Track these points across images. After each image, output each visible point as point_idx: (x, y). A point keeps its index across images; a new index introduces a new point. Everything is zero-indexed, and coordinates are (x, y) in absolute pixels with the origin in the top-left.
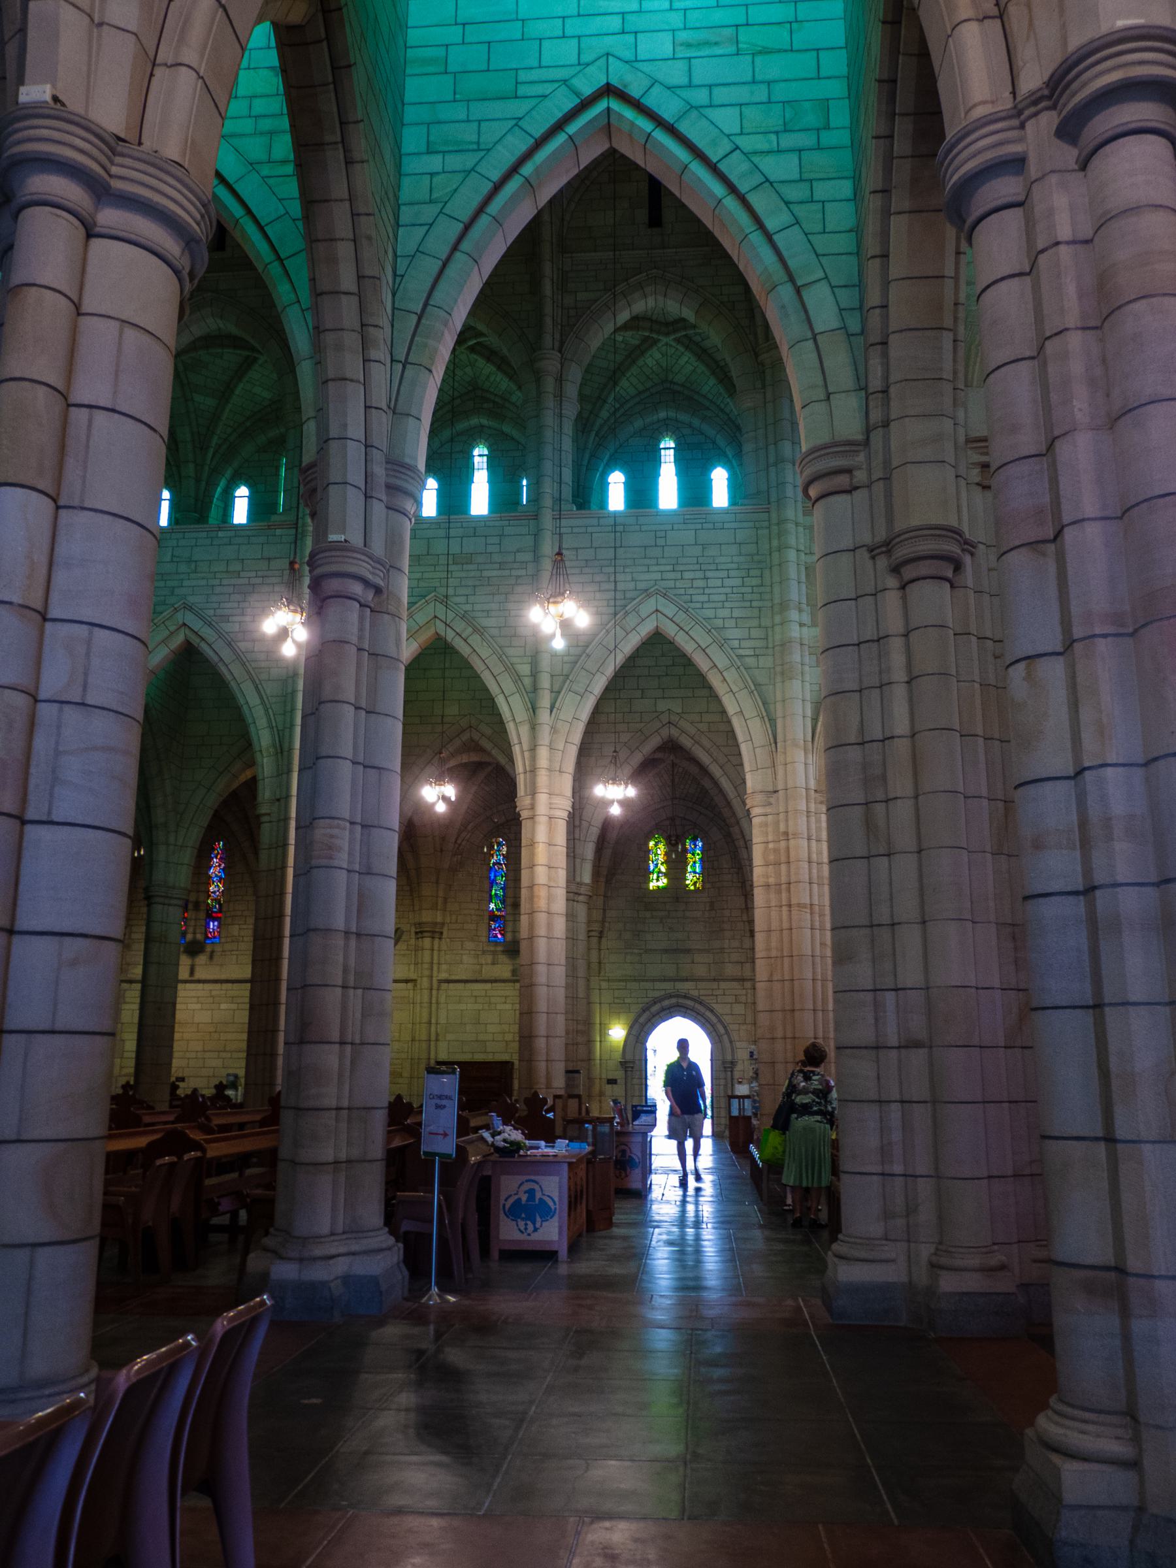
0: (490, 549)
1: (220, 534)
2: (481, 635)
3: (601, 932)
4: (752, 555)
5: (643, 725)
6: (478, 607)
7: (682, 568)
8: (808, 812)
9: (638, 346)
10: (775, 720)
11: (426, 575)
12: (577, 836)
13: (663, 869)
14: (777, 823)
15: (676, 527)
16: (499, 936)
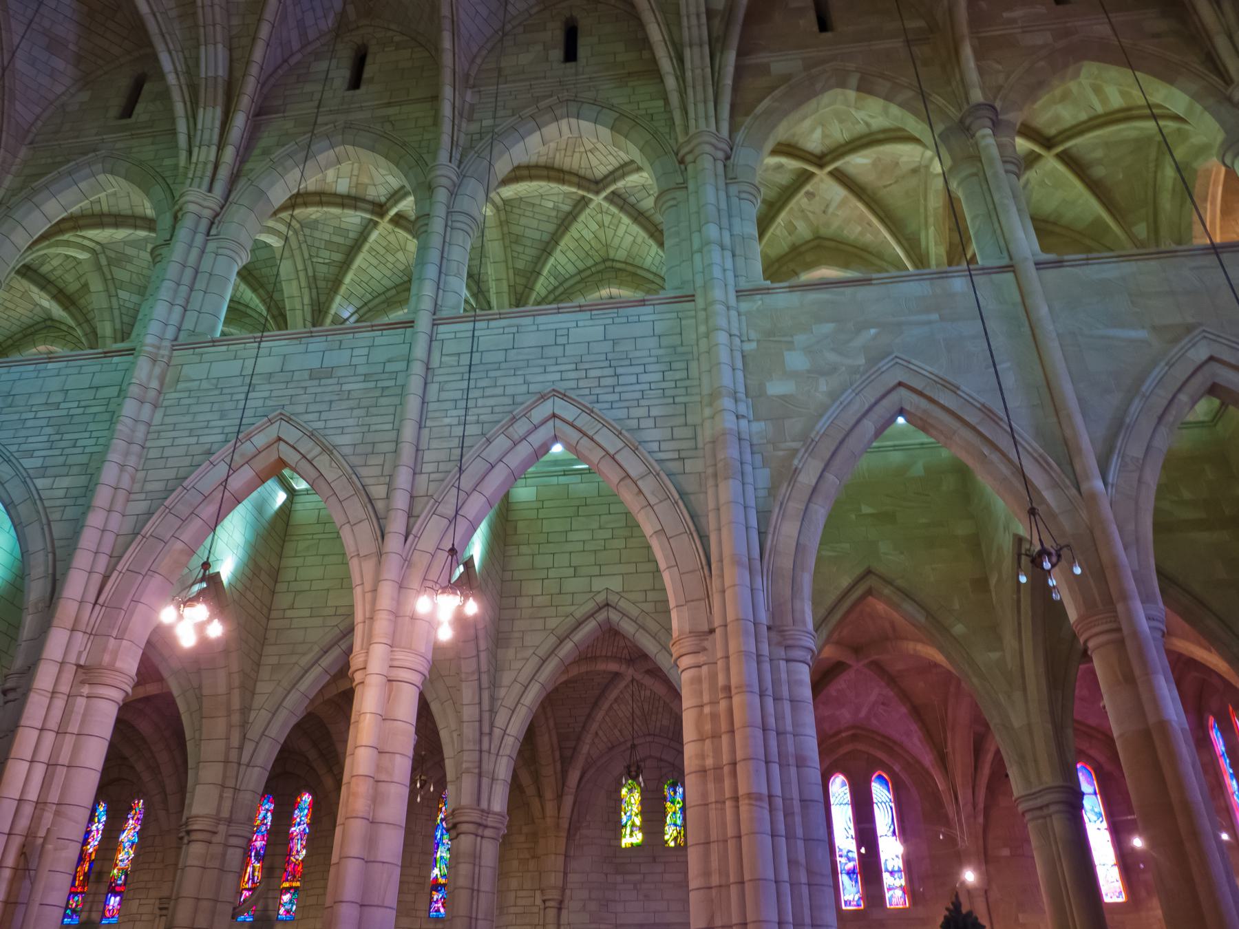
0: (354, 361)
1: (50, 366)
2: (330, 453)
3: (561, 902)
4: (674, 347)
5: (573, 608)
6: (330, 424)
7: (587, 366)
8: (758, 656)
9: (570, 213)
10: (708, 537)
11: (275, 393)
12: (485, 746)
13: (638, 821)
14: (713, 677)
15: (580, 324)
16: (442, 910)
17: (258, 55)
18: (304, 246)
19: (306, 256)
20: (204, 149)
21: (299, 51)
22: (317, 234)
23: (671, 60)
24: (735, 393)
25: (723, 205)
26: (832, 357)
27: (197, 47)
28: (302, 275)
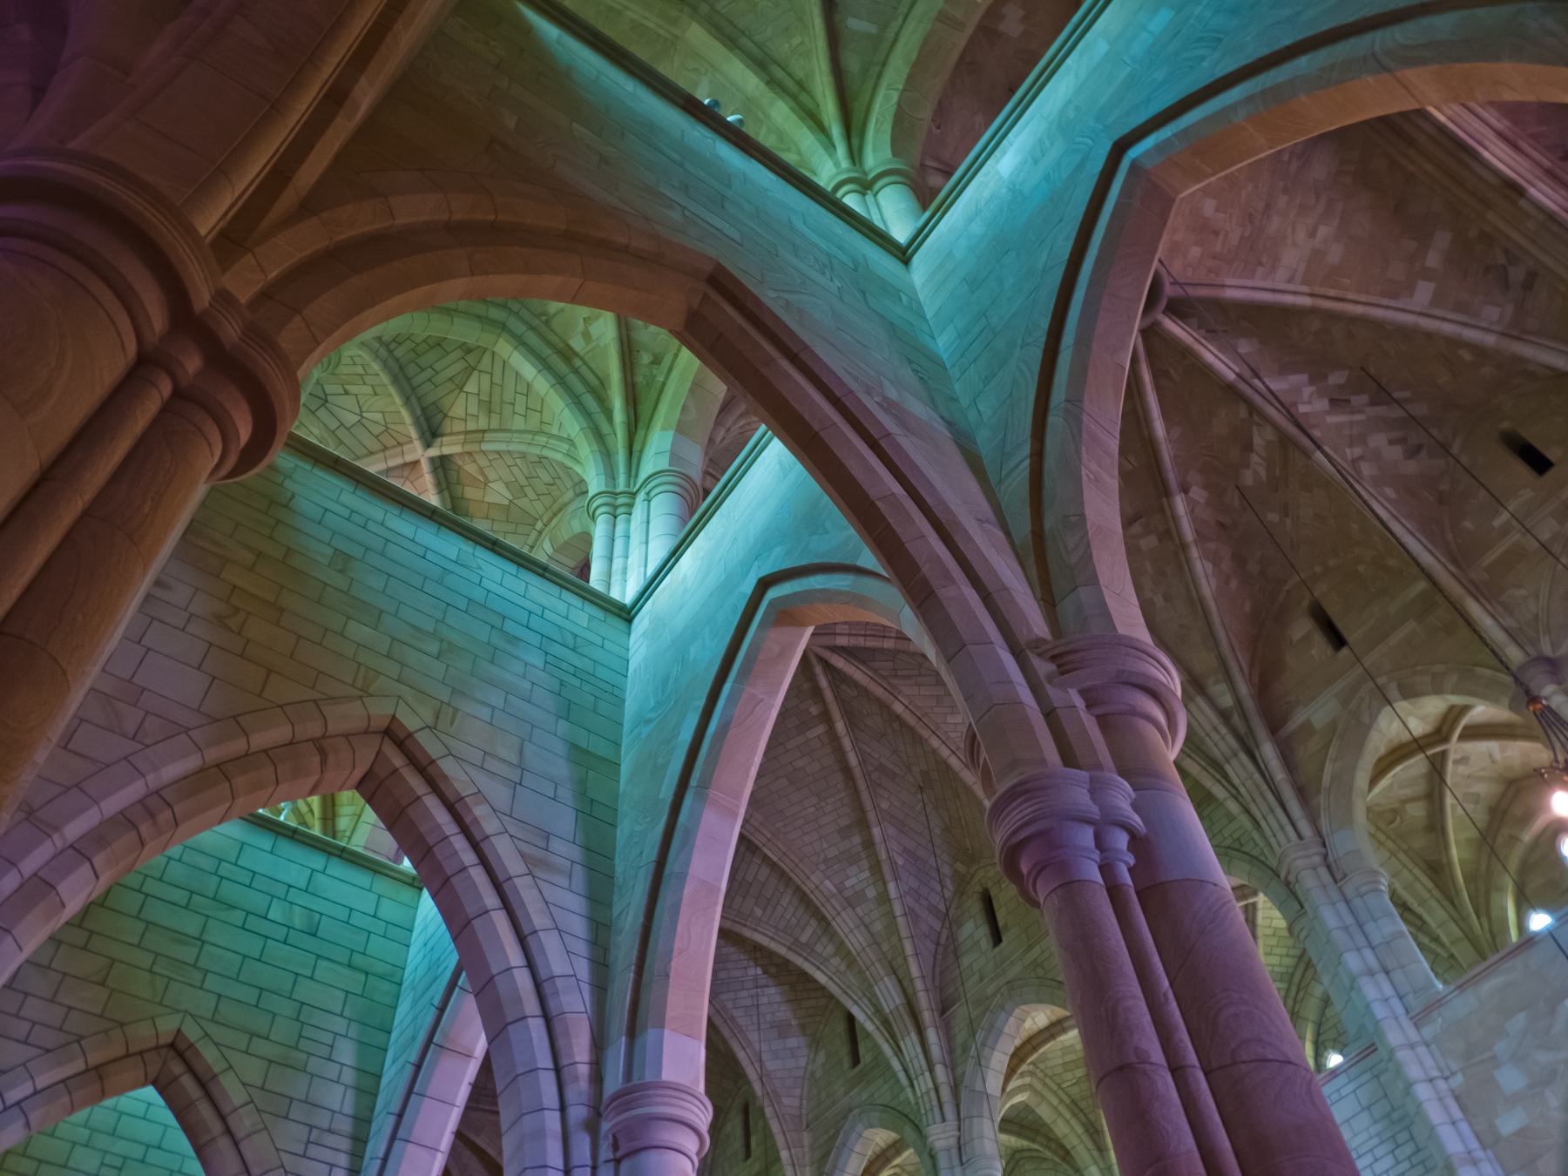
4: (1387, 1116)
17: (915, 971)
18: (1048, 1081)
19: (1055, 1088)
20: (920, 1078)
21: (943, 927)
22: (1049, 1064)
23: (1220, 782)
24: (1469, 1153)
25: (1349, 920)
26: (1543, 1057)
27: (871, 986)
28: (1062, 1108)
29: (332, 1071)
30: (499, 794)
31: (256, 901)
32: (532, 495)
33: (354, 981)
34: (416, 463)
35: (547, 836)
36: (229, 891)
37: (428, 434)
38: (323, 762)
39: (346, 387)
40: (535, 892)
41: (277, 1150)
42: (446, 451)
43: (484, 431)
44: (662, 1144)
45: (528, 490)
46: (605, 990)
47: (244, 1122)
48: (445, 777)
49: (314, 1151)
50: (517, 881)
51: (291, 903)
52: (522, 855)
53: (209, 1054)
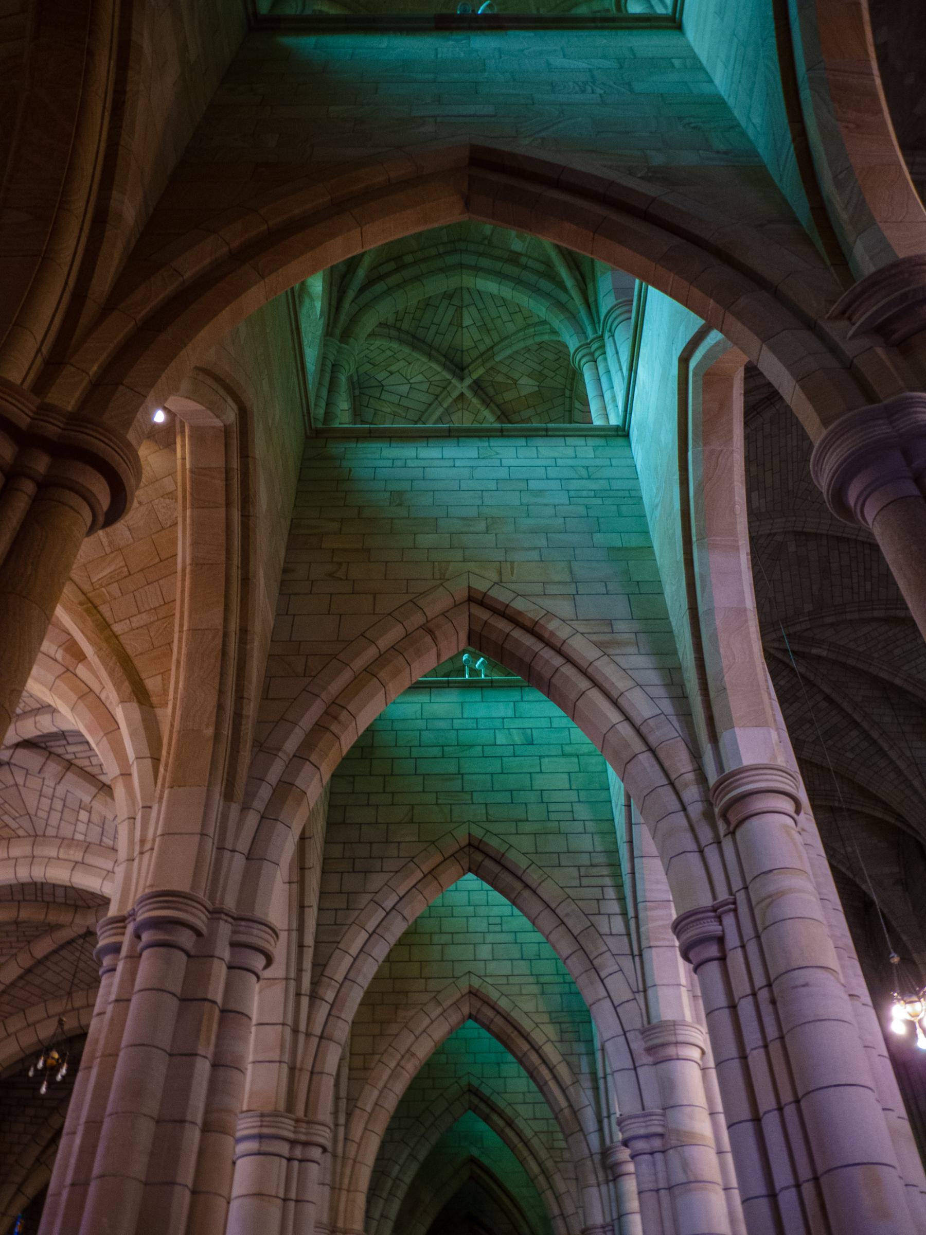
29: (578, 827)
30: (564, 608)
31: (485, 736)
32: (551, 374)
33: (570, 764)
34: (462, 394)
35: (610, 622)
36: (465, 737)
37: (458, 371)
38: (434, 639)
39: (388, 369)
40: (613, 666)
41: (561, 888)
42: (475, 376)
43: (492, 347)
44: (759, 811)
45: (546, 372)
46: (690, 715)
47: (533, 877)
48: (520, 613)
49: (585, 881)
50: (597, 663)
51: (509, 729)
52: (595, 644)
53: (494, 842)
